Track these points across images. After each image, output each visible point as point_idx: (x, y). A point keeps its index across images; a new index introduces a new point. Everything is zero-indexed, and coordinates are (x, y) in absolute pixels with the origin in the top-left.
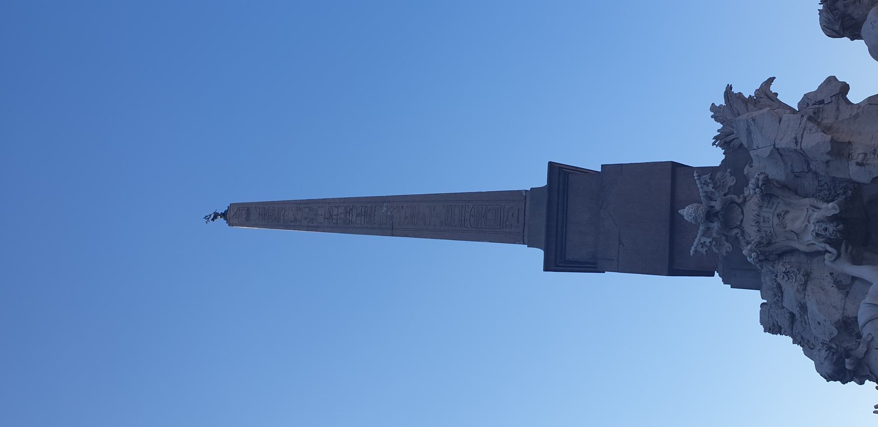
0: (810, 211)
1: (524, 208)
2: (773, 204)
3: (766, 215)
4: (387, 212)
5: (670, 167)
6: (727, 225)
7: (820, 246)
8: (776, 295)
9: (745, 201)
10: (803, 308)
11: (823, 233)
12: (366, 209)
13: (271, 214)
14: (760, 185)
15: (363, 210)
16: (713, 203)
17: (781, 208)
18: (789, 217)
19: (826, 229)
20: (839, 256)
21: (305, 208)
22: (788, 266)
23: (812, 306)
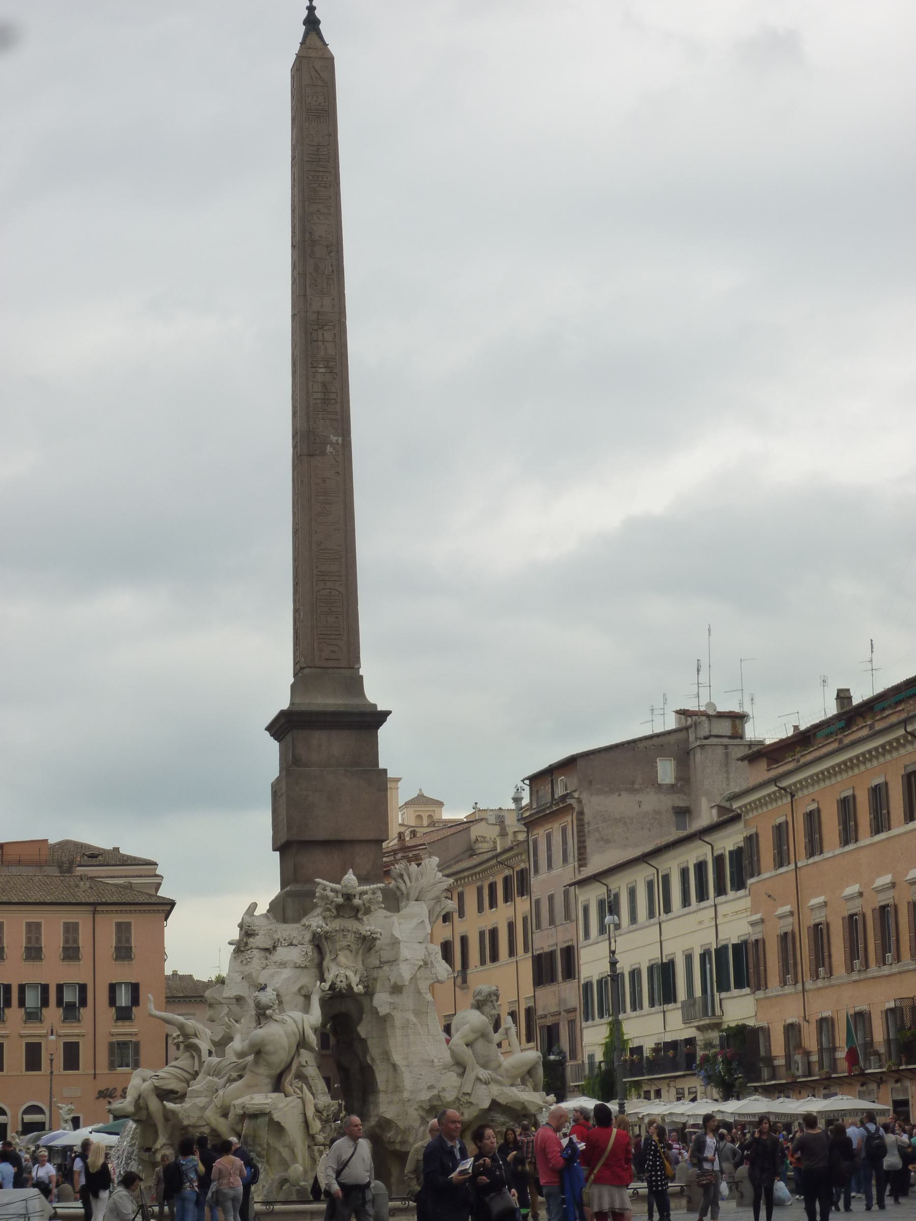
0: (353, 969)
1: (341, 666)
2: (357, 941)
3: (349, 936)
4: (331, 443)
5: (383, 838)
6: (339, 907)
7: (330, 977)
8: (285, 940)
9: (358, 919)
10: (283, 965)
11: (339, 979)
12: (333, 402)
13: (320, 179)
14: (372, 935)
15: (333, 396)
16: (357, 897)
17: (354, 947)
18: (348, 952)
19: (341, 982)
20: (324, 991)
21: (332, 265)
22: (311, 954)
23: (287, 973)
